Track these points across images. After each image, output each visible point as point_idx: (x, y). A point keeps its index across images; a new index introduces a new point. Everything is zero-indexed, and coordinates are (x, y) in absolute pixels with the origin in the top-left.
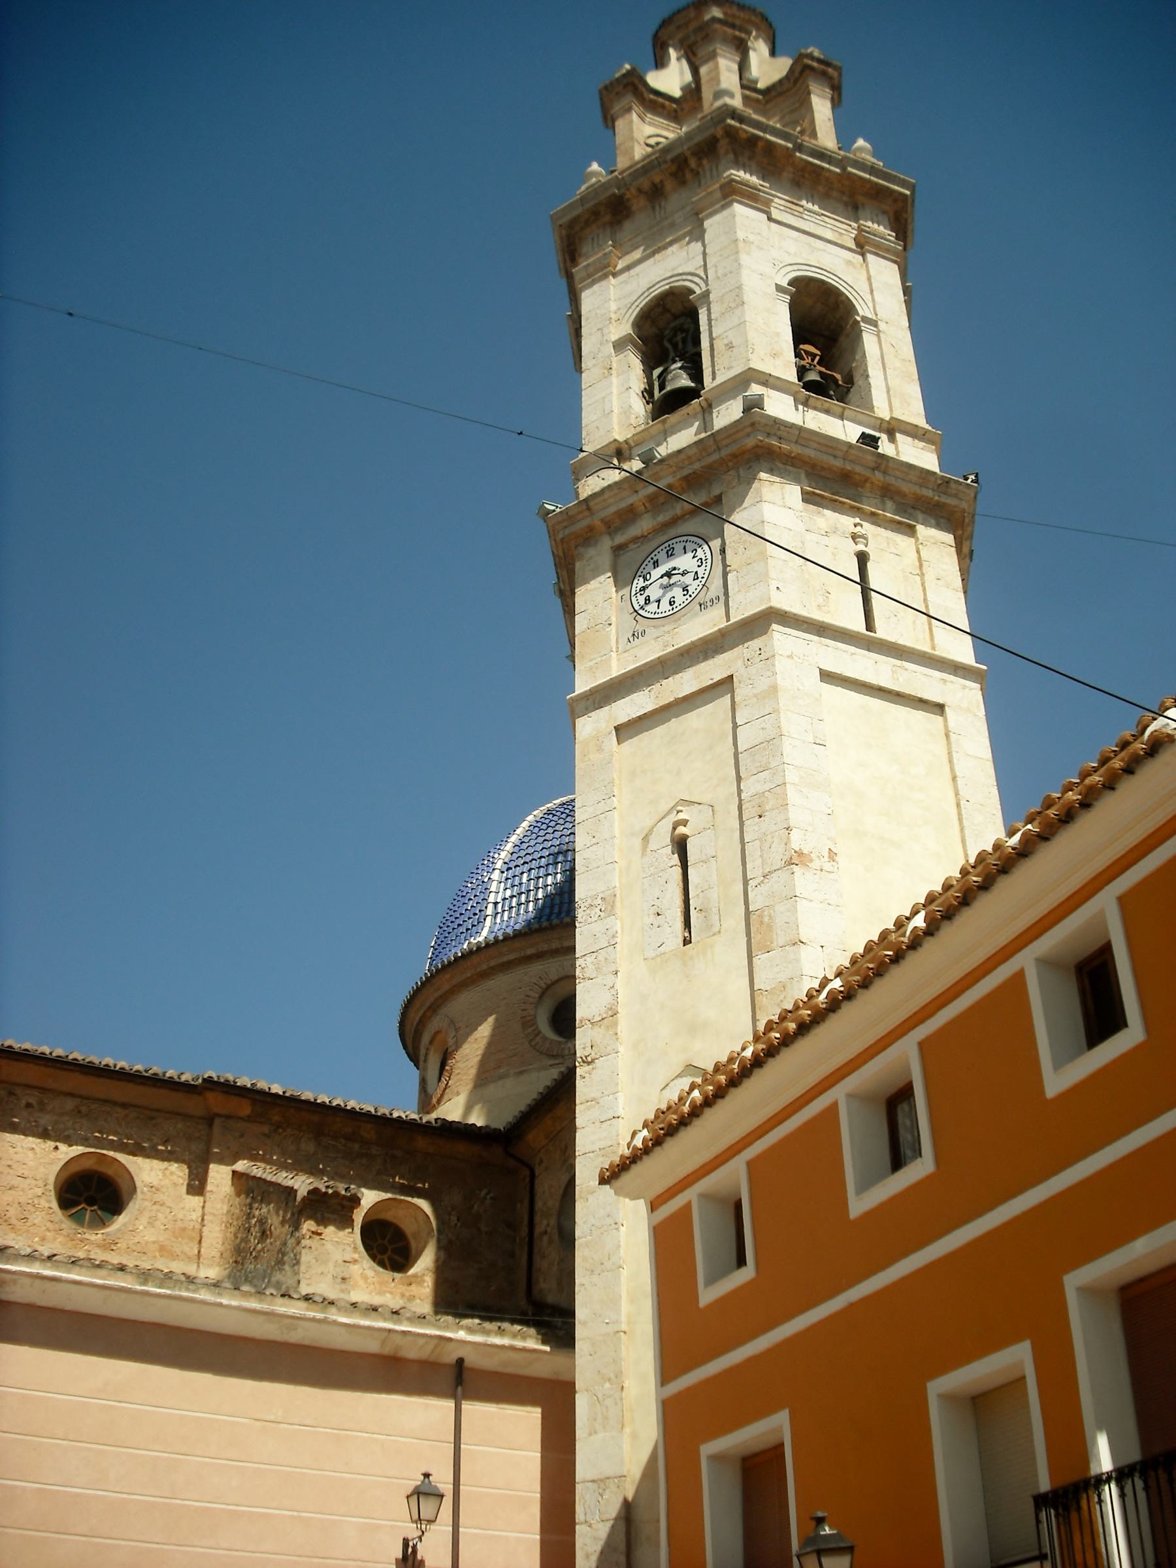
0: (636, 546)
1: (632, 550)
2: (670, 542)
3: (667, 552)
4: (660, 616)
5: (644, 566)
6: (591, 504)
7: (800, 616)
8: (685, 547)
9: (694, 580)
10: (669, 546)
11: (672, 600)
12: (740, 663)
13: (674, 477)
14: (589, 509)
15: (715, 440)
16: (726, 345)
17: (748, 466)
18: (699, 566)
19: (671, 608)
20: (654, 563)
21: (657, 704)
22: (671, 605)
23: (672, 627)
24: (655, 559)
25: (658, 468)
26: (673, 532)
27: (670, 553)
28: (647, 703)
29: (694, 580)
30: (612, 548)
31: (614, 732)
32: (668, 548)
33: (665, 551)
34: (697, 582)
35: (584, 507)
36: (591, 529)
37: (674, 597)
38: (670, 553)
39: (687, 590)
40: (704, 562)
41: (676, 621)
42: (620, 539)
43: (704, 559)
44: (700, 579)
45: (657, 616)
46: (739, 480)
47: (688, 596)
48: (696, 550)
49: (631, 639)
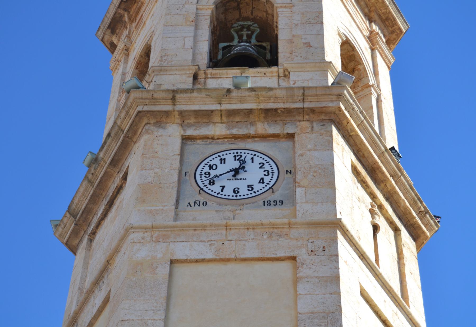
0: (203, 143)
1: (198, 144)
2: (239, 151)
3: (235, 156)
4: (223, 196)
5: (228, 152)
6: (178, 96)
7: (354, 239)
8: (252, 159)
9: (259, 182)
10: (237, 153)
11: (236, 189)
12: (304, 251)
13: (258, 106)
14: (173, 98)
15: (303, 94)
16: (306, 43)
17: (322, 124)
18: (265, 175)
19: (235, 195)
20: (221, 160)
21: (216, 256)
22: (234, 191)
23: (234, 208)
24: (223, 157)
25: (247, 93)
26: (242, 145)
27: (237, 158)
28: (207, 252)
29: (259, 182)
30: (182, 136)
31: (169, 263)
32: (235, 154)
33: (234, 155)
34: (262, 185)
35: (171, 96)
36: (167, 114)
37: (238, 189)
38: (237, 158)
39: (253, 189)
40: (271, 174)
41: (240, 205)
42: (190, 132)
43: (270, 171)
44: (265, 184)
45: (219, 196)
46: (312, 130)
47: (252, 192)
48: (264, 164)
49: (192, 204)
